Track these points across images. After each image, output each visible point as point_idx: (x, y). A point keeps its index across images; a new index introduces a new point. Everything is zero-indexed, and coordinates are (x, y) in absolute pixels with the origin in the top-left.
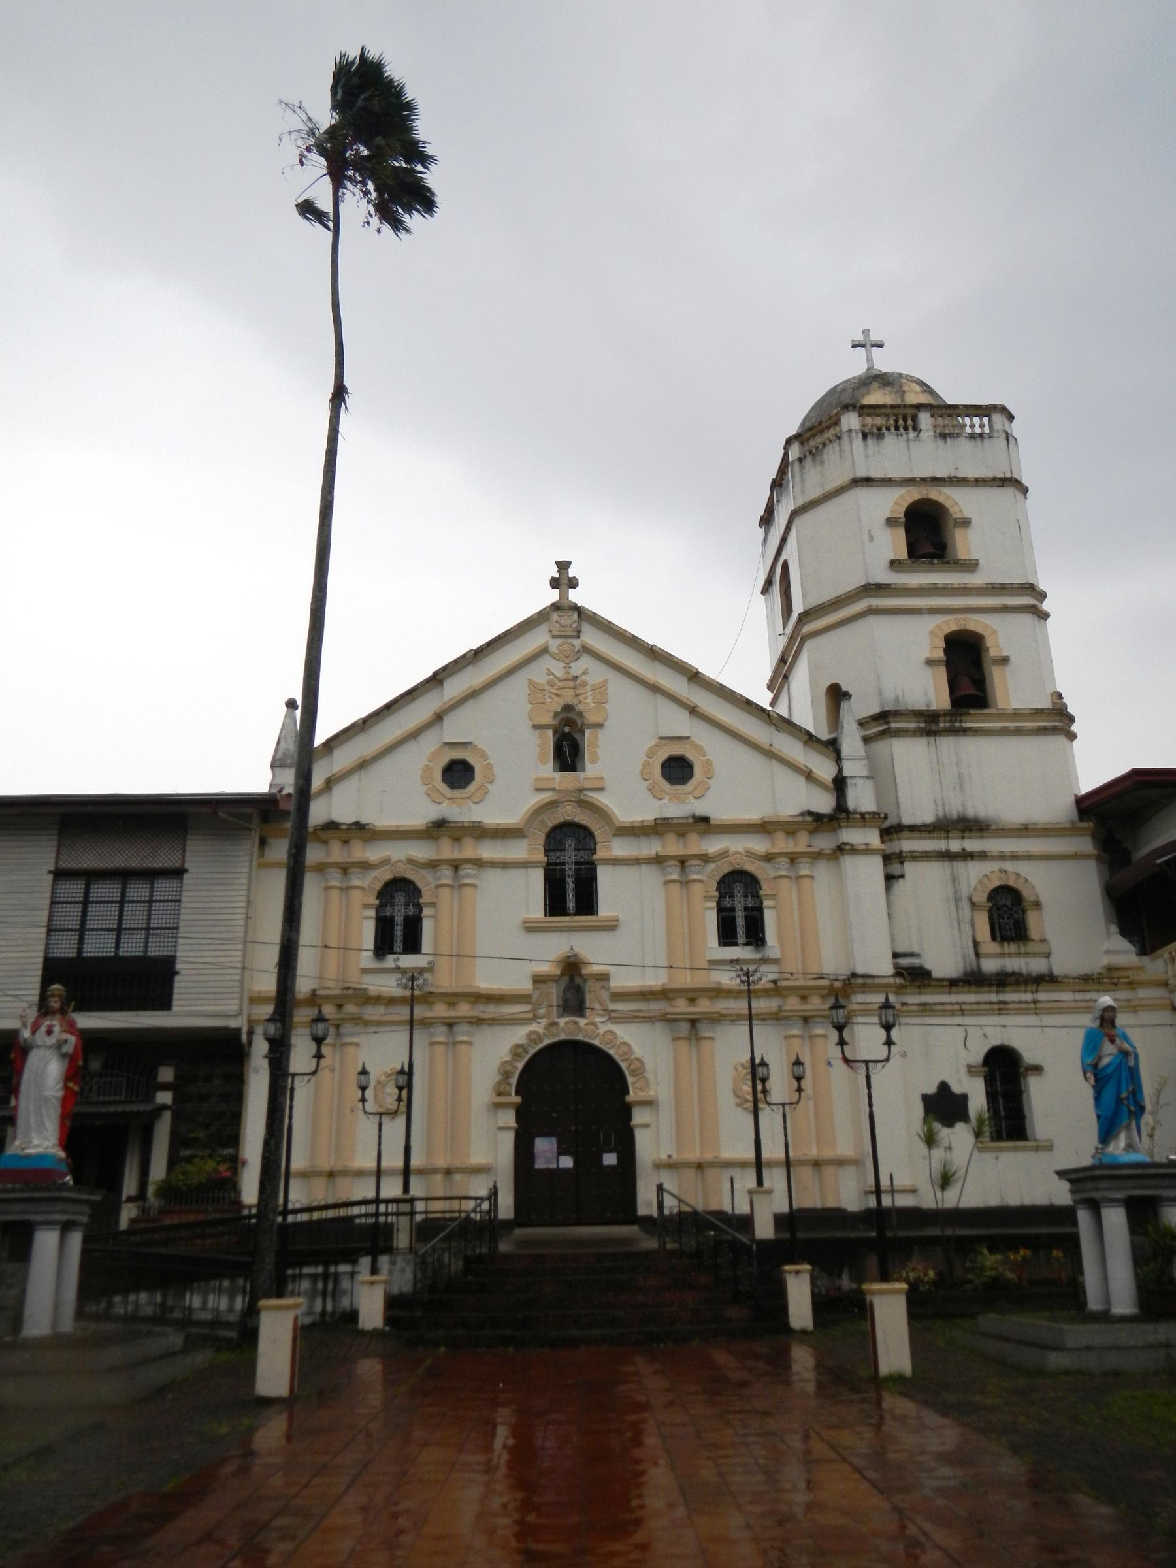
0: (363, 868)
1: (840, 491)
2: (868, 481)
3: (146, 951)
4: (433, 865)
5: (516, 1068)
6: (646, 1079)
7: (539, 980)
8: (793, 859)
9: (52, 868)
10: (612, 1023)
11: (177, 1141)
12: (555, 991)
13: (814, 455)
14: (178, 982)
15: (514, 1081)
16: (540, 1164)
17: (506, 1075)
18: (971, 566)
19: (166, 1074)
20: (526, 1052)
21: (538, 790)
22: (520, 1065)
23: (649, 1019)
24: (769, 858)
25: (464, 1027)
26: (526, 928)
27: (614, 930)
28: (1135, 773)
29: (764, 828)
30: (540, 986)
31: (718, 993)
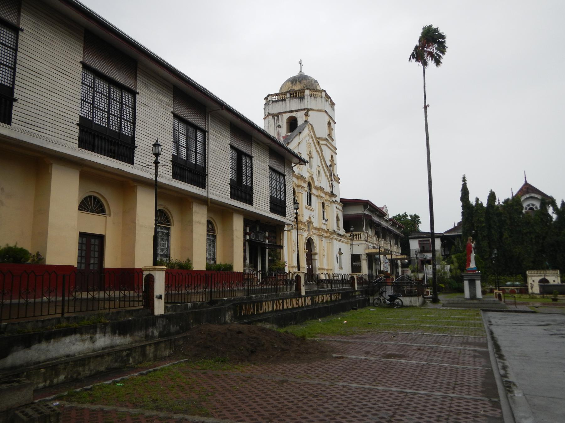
1: (321, 111)
2: (326, 112)
3: (280, 198)
4: (298, 186)
8: (329, 201)
11: (270, 255)
13: (314, 97)
17: (305, 244)
18: (333, 140)
19: (267, 234)
21: (308, 172)
23: (316, 234)
24: (326, 201)
28: (368, 200)
29: (326, 193)
31: (323, 230)
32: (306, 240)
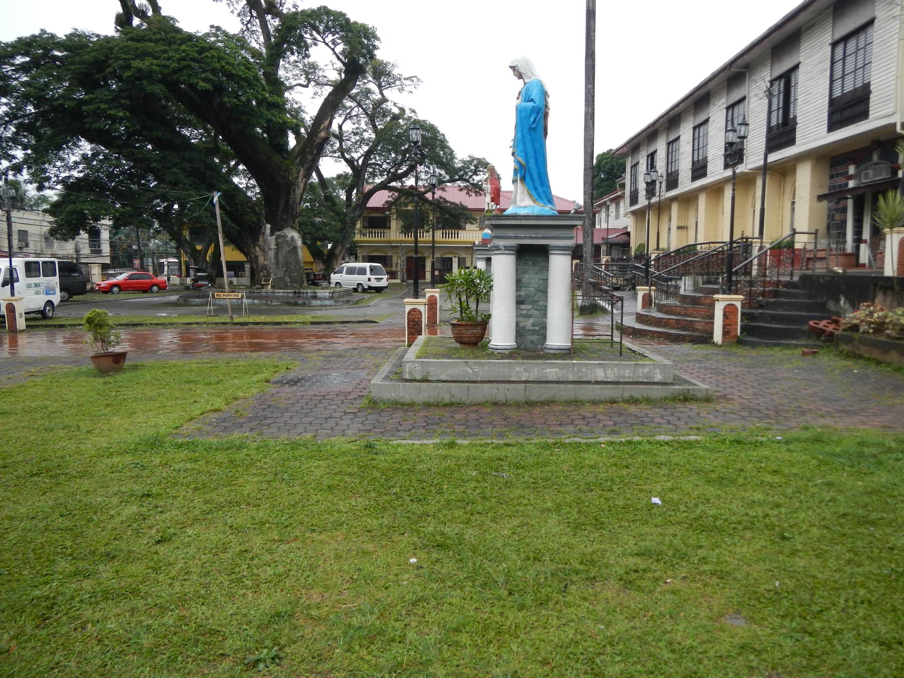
9: (830, 41)
14: (873, 98)
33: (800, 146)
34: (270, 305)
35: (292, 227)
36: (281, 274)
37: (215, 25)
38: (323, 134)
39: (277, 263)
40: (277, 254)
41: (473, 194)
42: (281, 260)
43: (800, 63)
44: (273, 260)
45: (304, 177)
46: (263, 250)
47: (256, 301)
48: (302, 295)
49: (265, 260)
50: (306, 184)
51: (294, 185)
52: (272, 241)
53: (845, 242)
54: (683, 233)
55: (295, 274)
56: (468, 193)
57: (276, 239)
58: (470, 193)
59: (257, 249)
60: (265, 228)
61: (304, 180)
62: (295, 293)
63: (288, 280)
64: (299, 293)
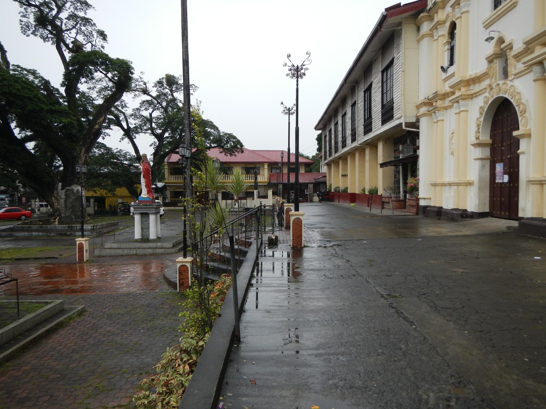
0: (440, 24)
5: (481, 122)
6: (524, 117)
7: (490, 60)
9: (381, 70)
10: (517, 78)
12: (497, 64)
15: (480, 130)
16: (497, 181)
17: (478, 126)
20: (484, 111)
22: (482, 119)
25: (461, 102)
26: (484, 27)
27: (515, 6)
30: (492, 64)
32: (481, 114)
33: (375, 131)
34: (49, 236)
35: (77, 184)
36: (68, 213)
37: (15, 64)
38: (97, 127)
39: (66, 206)
40: (66, 202)
41: (229, 155)
42: (69, 205)
43: (372, 82)
44: (63, 205)
45: (85, 153)
46: (56, 199)
47: (40, 233)
48: (73, 228)
49: (58, 205)
50: (86, 157)
51: (78, 158)
52: (62, 194)
53: (399, 192)
54: (344, 178)
55: (79, 213)
56: (225, 154)
57: (66, 192)
58: (227, 154)
59: (53, 198)
60: (58, 185)
61: (85, 155)
62: (69, 227)
63: (73, 217)
64: (72, 227)
